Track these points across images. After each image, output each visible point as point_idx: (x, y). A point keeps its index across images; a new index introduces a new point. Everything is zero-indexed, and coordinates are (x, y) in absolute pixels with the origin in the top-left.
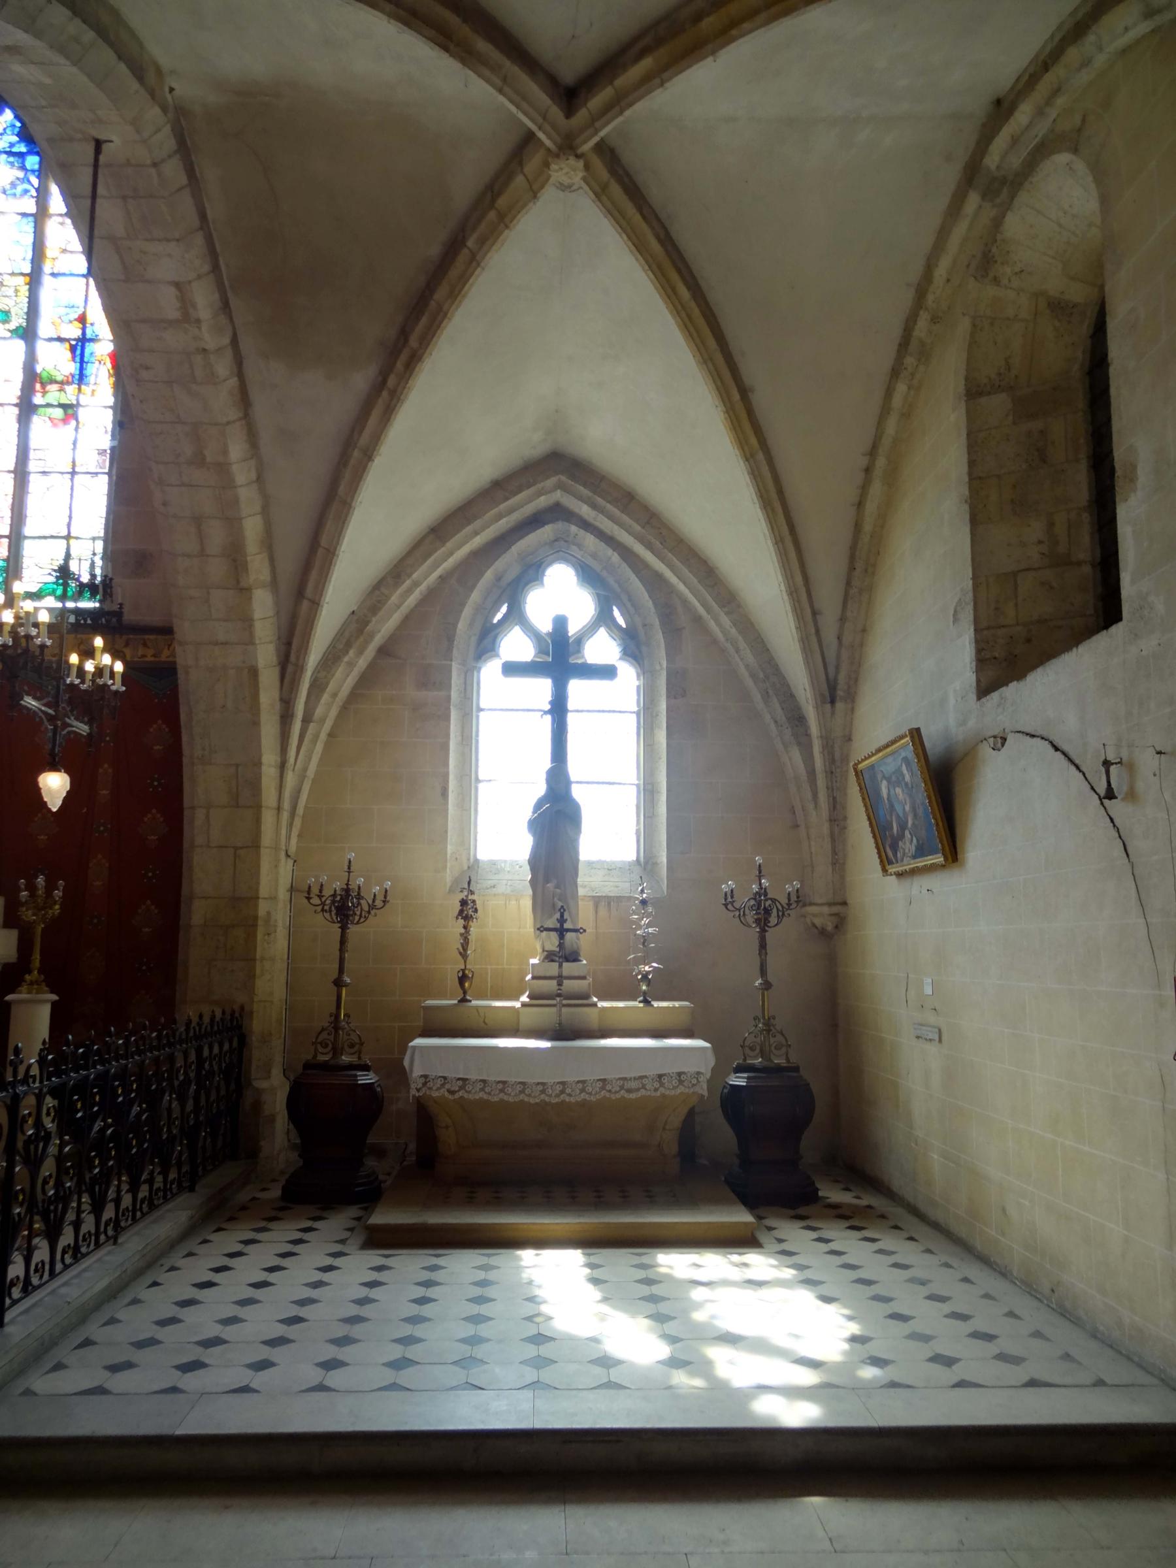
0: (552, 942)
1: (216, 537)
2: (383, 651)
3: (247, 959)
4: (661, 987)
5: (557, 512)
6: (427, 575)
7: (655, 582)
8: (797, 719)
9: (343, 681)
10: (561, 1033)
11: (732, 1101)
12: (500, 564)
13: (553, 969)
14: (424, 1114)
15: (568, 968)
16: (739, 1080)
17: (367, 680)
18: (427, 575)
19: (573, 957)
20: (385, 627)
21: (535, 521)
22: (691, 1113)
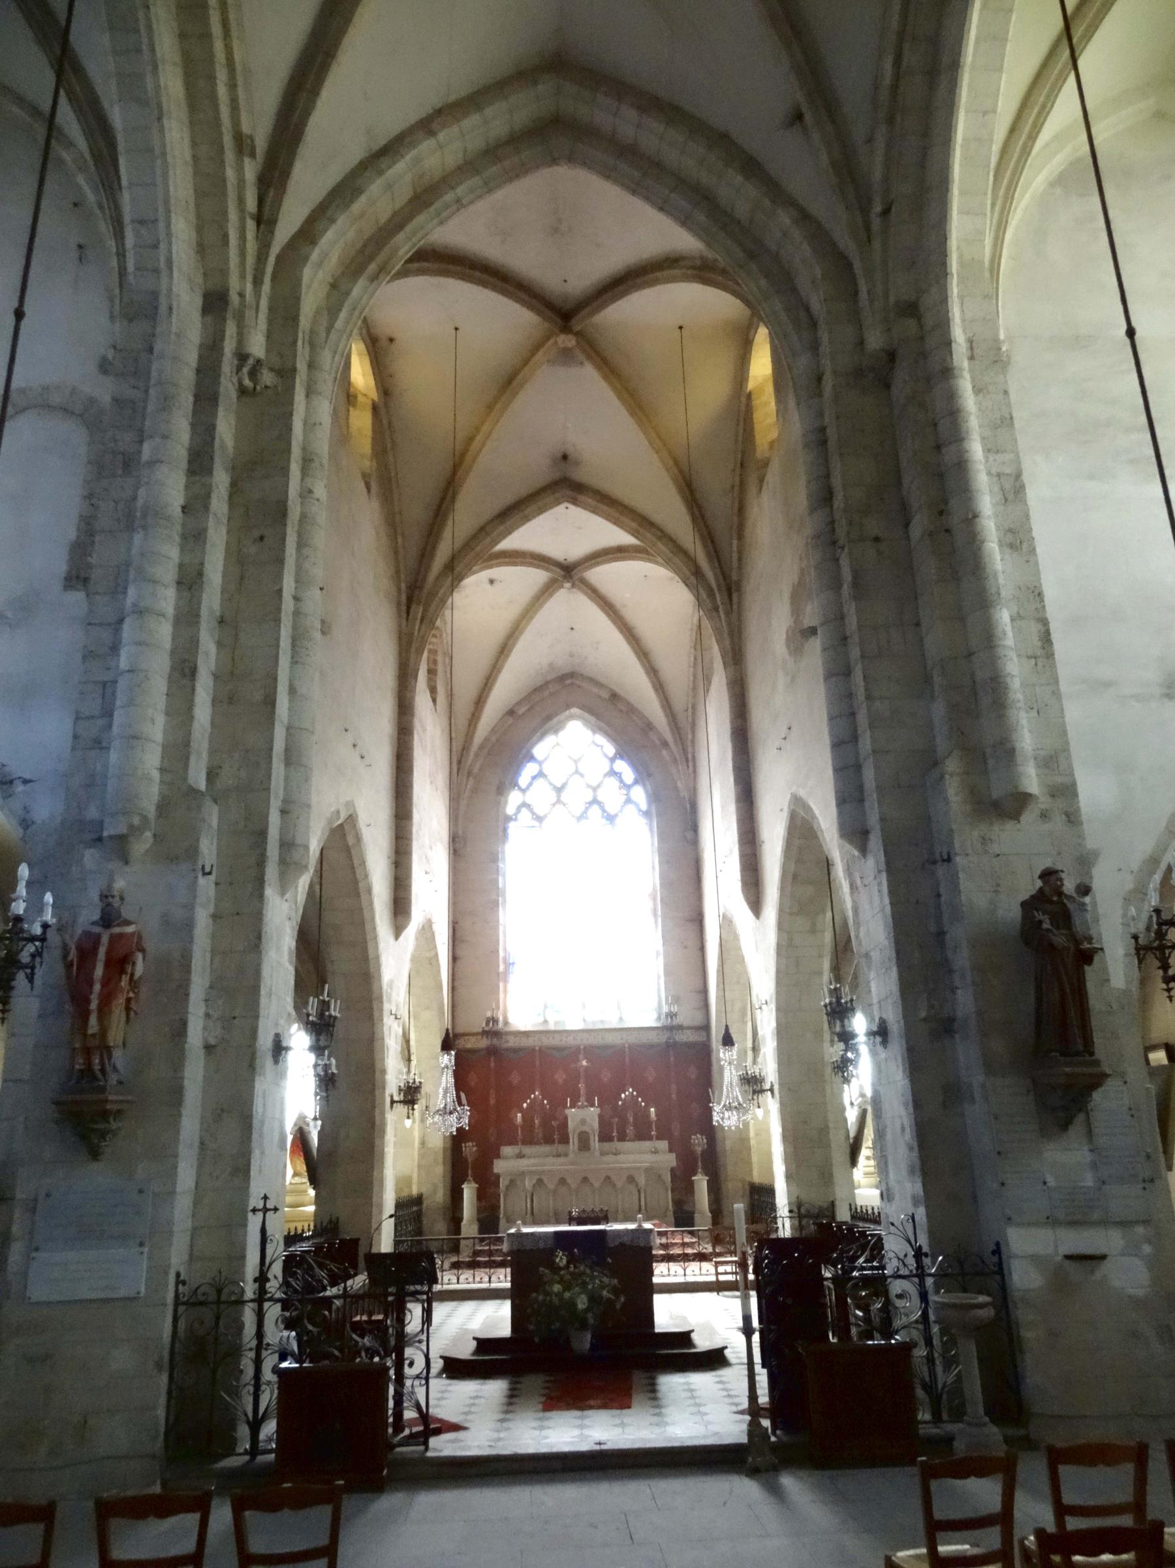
1: (738, 1006)
3: (750, 1163)
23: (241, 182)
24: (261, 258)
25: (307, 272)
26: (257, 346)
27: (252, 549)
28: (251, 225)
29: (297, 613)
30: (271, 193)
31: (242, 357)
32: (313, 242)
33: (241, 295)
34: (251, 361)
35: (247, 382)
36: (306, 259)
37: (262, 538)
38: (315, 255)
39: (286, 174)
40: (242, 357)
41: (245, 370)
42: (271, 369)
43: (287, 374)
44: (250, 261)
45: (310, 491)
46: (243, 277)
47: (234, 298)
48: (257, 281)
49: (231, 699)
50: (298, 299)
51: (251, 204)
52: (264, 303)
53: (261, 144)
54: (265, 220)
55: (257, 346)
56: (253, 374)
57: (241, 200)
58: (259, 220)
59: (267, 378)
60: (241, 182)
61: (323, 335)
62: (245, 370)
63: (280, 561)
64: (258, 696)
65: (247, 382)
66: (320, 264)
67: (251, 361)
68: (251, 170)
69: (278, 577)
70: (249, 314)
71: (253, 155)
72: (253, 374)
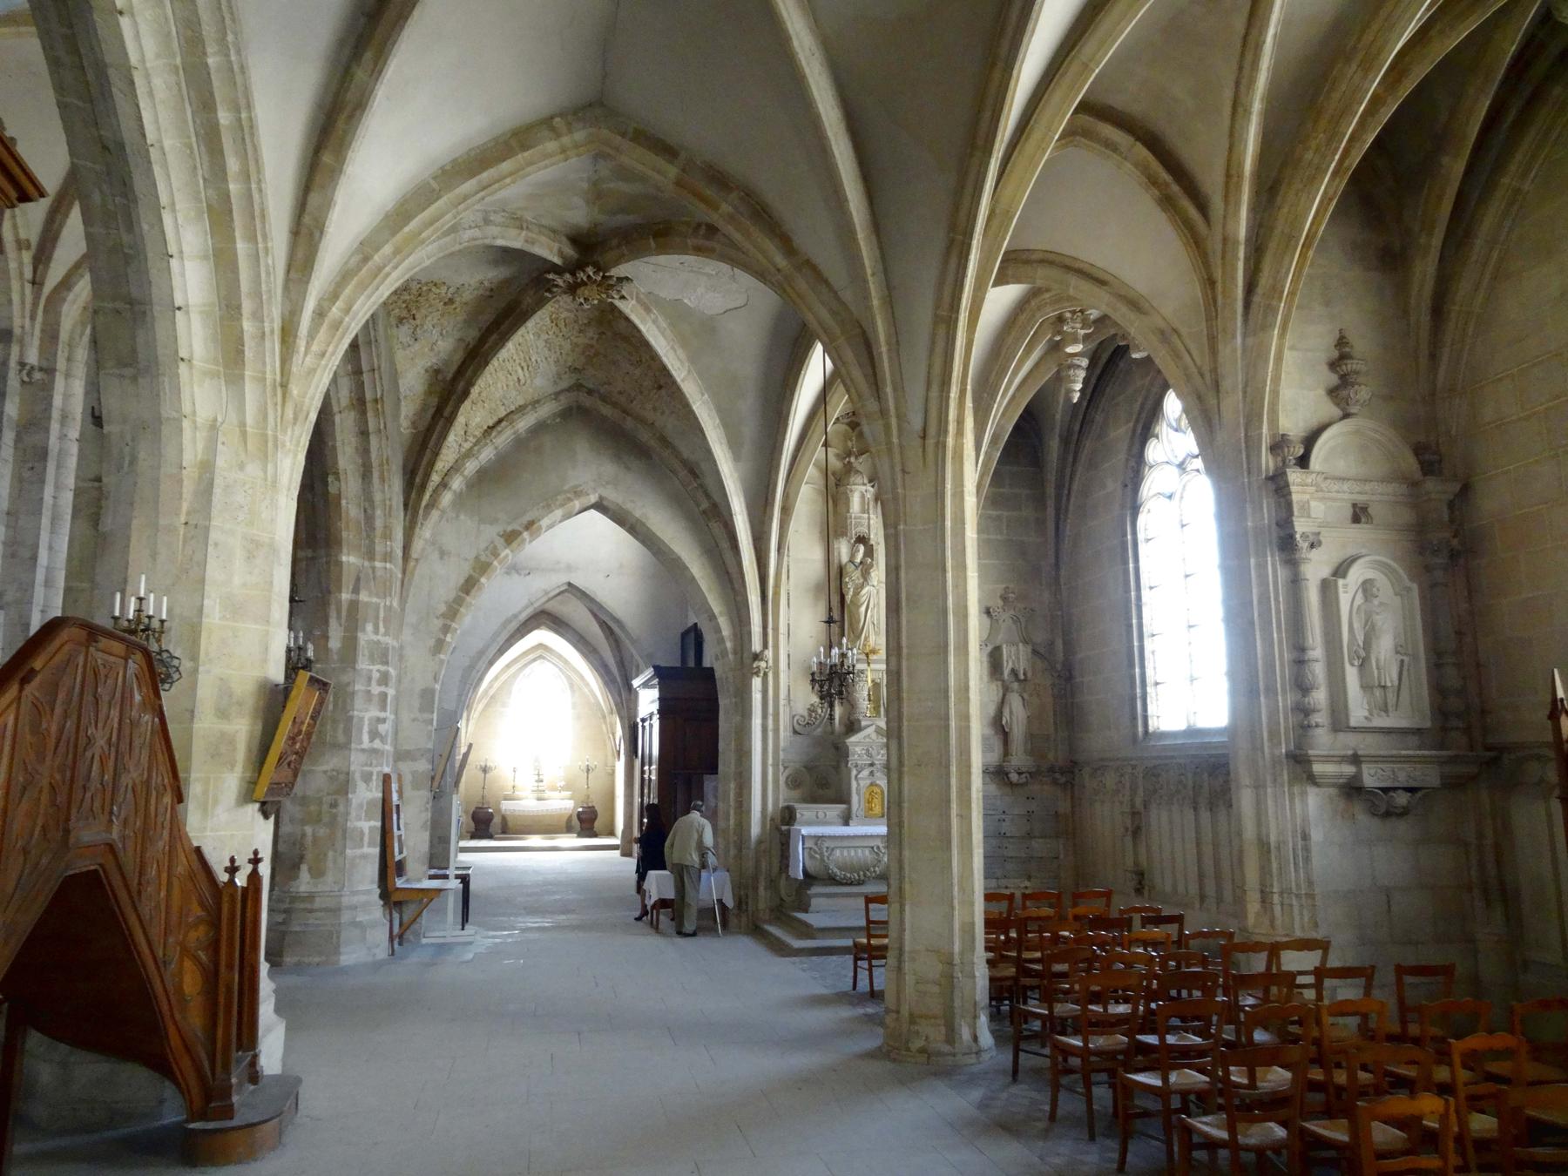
0: (536, 778)
2: (492, 697)
4: (563, 789)
5: (541, 657)
6: (503, 678)
7: (568, 678)
8: (604, 717)
9: (481, 707)
10: (539, 799)
11: (579, 814)
12: (524, 672)
13: (536, 784)
14: (504, 818)
15: (541, 784)
16: (580, 810)
17: (487, 706)
18: (503, 678)
19: (542, 781)
20: (491, 692)
21: (534, 660)
22: (569, 819)
23: (21, 264)
24: (35, 305)
25: (65, 308)
26: (33, 357)
27: (27, 474)
28: (28, 288)
29: (55, 505)
30: (41, 267)
31: (22, 364)
32: (69, 289)
33: (23, 327)
34: (28, 367)
35: (26, 379)
36: (64, 300)
37: (32, 468)
38: (71, 297)
39: (49, 259)
40: (22, 364)
41: (25, 372)
42: (41, 369)
43: (50, 371)
44: (28, 306)
45: (66, 435)
46: (23, 317)
47: (17, 331)
48: (33, 318)
49: (13, 556)
50: (58, 324)
51: (28, 274)
52: (37, 332)
53: (34, 240)
54: (37, 283)
55: (33, 357)
56: (29, 374)
57: (21, 274)
58: (33, 283)
59: (37, 375)
60: (21, 264)
61: (77, 338)
62: (25, 372)
63: (42, 482)
64: (28, 554)
65: (26, 379)
66: (74, 301)
67: (28, 367)
68: (27, 257)
69: (42, 489)
70: (27, 339)
71: (28, 247)
72: (29, 374)
